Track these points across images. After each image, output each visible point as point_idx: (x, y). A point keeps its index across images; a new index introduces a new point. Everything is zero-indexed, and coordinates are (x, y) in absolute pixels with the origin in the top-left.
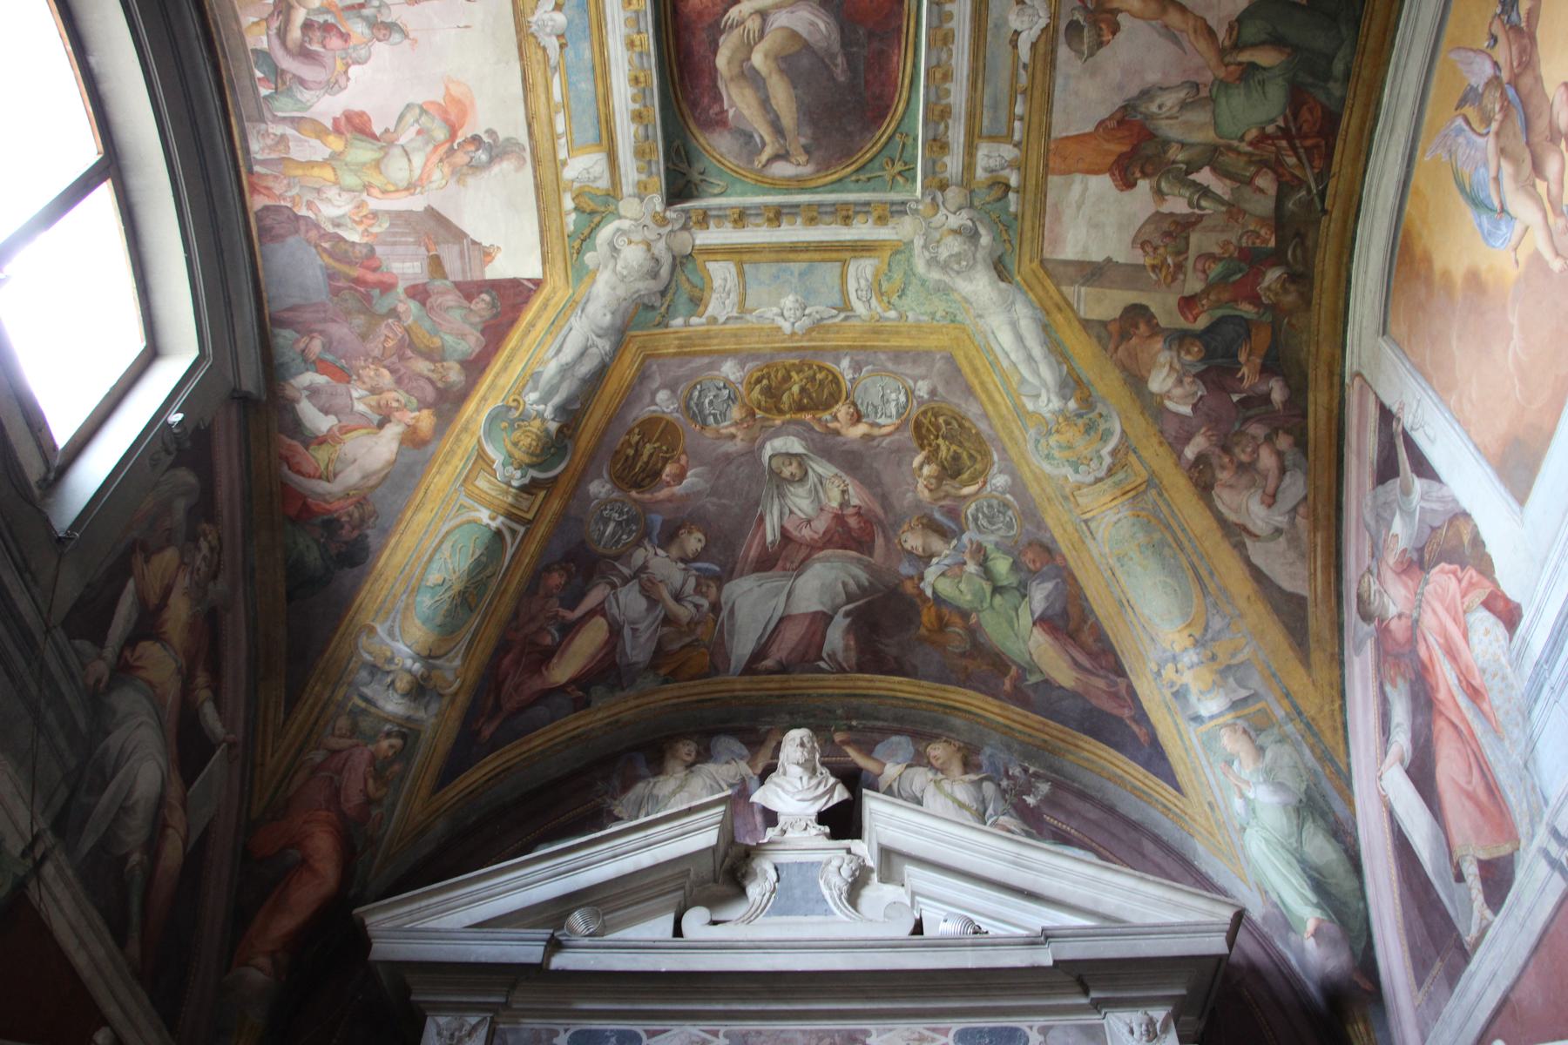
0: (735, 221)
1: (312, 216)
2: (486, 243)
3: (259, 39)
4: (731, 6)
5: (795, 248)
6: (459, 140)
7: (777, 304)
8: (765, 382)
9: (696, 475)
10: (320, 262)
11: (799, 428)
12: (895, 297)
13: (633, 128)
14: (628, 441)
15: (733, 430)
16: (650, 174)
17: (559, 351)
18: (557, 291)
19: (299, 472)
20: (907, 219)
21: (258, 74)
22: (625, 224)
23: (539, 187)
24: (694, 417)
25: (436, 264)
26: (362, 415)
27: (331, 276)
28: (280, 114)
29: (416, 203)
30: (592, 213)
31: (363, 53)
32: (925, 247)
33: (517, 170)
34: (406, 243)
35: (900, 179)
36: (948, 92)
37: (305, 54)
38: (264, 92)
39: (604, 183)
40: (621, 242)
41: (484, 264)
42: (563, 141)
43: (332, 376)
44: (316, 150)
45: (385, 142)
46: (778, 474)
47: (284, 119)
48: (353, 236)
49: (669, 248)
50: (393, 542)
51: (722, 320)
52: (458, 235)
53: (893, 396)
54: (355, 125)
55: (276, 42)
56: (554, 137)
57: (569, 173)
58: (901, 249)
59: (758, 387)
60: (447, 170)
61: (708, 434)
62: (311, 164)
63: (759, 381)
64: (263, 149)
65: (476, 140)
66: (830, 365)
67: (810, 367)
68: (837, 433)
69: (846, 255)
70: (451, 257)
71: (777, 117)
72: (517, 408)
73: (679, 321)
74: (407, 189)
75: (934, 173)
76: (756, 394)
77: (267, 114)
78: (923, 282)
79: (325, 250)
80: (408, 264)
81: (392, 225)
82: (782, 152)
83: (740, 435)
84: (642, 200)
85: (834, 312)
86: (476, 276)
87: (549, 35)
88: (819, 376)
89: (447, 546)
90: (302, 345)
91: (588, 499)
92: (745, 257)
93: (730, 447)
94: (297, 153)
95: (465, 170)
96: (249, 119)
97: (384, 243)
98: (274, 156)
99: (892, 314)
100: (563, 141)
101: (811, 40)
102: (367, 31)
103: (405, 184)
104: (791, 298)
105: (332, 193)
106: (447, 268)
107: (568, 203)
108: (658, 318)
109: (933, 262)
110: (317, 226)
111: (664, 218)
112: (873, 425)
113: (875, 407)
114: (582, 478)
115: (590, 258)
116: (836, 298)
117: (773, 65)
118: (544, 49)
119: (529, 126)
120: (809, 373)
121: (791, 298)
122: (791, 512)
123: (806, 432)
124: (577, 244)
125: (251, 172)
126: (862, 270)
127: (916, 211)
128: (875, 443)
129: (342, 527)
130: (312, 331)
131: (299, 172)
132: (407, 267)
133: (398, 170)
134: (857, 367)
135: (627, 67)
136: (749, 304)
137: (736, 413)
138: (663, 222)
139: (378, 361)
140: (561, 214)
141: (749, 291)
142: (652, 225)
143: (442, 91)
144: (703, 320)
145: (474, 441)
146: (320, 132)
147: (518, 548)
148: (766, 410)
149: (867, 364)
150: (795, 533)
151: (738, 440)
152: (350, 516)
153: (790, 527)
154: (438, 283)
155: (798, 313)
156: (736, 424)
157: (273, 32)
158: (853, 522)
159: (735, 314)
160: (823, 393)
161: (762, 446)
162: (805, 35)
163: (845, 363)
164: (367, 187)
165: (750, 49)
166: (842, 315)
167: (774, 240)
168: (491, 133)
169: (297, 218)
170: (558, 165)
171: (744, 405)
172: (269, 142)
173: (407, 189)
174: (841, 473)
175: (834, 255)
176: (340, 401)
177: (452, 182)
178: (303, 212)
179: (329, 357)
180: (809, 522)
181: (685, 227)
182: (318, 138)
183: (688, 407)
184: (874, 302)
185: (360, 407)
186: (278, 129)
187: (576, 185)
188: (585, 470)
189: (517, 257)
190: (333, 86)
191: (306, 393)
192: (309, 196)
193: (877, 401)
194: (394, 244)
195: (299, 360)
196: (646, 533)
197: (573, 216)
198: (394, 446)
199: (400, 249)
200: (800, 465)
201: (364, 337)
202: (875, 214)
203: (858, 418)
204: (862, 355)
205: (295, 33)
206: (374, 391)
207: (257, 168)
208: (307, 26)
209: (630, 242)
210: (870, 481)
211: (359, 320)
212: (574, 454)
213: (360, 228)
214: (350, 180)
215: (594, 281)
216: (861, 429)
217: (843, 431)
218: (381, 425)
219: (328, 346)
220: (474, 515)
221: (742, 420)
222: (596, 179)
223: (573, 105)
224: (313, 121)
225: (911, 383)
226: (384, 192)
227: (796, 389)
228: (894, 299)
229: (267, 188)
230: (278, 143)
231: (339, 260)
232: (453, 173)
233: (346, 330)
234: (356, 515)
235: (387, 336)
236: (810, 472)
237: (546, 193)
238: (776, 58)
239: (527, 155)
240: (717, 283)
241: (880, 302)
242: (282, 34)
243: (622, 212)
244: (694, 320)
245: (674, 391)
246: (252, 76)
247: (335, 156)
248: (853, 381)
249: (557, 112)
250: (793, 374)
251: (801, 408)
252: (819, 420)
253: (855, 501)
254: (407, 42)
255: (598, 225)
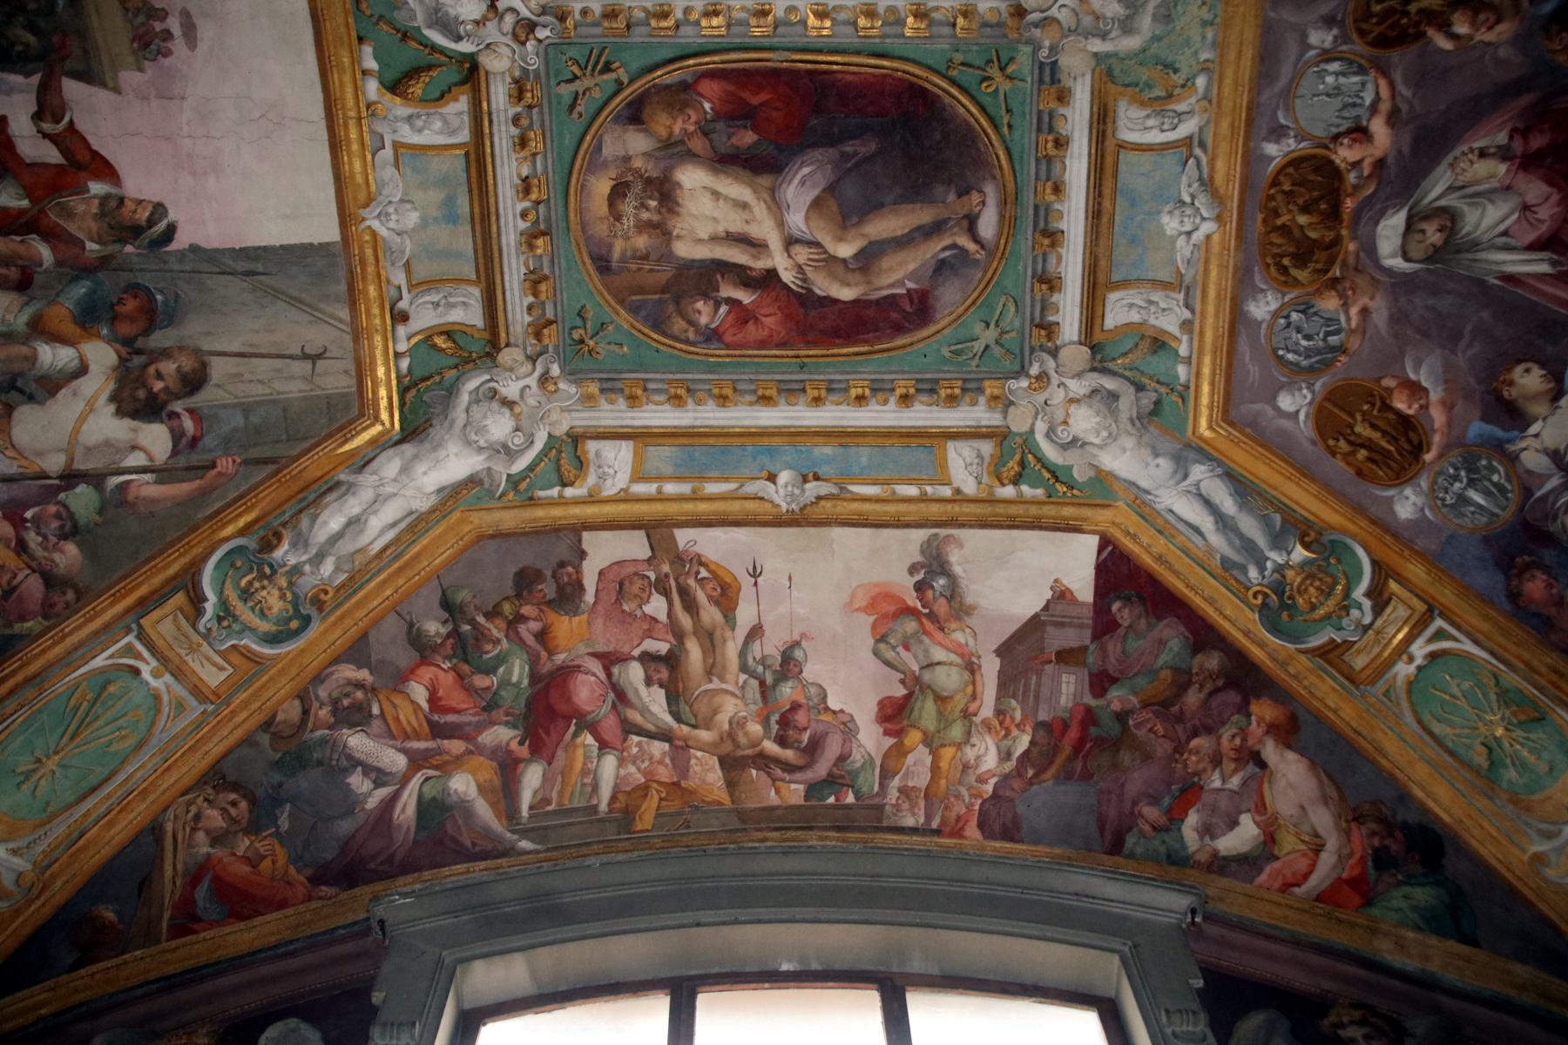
0: (1051, 289)
1: (993, 781)
2: (1049, 594)
3: (795, 792)
4: (780, 280)
5: (1096, 215)
6: (919, 605)
7: (1173, 240)
8: (1286, 262)
9: (1417, 366)
10: (1050, 783)
11: (1366, 216)
12: (1175, 77)
13: (918, 406)
14: (1346, 455)
15: (1354, 311)
16: (980, 391)
17: (1197, 530)
18: (1118, 518)
19: (1306, 876)
20: (1064, 61)
21: (832, 800)
22: (1041, 427)
23: (984, 524)
24: (1327, 365)
25: (1066, 657)
26: (1244, 783)
27: (1067, 776)
28: (876, 788)
29: (991, 667)
30: (1022, 464)
31: (813, 690)
32: (1104, 36)
33: (961, 545)
34: (1039, 684)
35: (1010, 70)
36: (891, 10)
37: (813, 749)
38: (850, 799)
39: (987, 447)
40: (1064, 435)
41: (1074, 601)
42: (929, 489)
43: (1190, 804)
44: (919, 759)
45: (916, 686)
46: (1437, 249)
47: (881, 784)
48: (1023, 742)
49: (1079, 375)
50: (1418, 793)
51: (1187, 314)
52: (1034, 624)
53: (1330, 79)
54: (894, 715)
55: (798, 776)
56: (923, 499)
57: (970, 488)
58: (1107, 73)
59: (1293, 272)
60: (954, 626)
61: (1354, 344)
62: (935, 768)
63: (1284, 270)
64: (914, 814)
65: (920, 587)
66: (1272, 168)
67: (1271, 198)
68: (1380, 163)
69: (1110, 145)
70: (1058, 639)
71: (919, 228)
72: (1266, 596)
73: (1182, 371)
74: (973, 672)
75: (1000, 25)
76: (1302, 275)
77: (876, 801)
78: (1156, 38)
79: (1036, 775)
80: (1064, 690)
81: (1014, 697)
82: (965, 223)
83: (1364, 301)
84: (1012, 403)
85: (1191, 161)
86: (1088, 615)
87: (803, 491)
88: (1287, 187)
89: (1438, 728)
90: (1147, 828)
91: (1419, 524)
92: (1101, 278)
93: (1380, 317)
94: (921, 779)
95: (955, 605)
96: (880, 820)
97: (1036, 710)
98: (922, 804)
99: (1201, 81)
100: (929, 489)
101: (823, 184)
102: (790, 684)
103: (966, 676)
104: (1165, 219)
105: (970, 753)
106: (1074, 644)
107: (1008, 491)
108: (1174, 398)
109: (1127, 26)
110: (1006, 778)
111: (1038, 378)
112: (1374, 109)
113: (1345, 106)
114: (1386, 527)
115: (1079, 475)
116: (1171, 160)
117: (853, 231)
118: (819, 498)
119: (907, 526)
120: (1280, 198)
121: (1165, 219)
122: (1505, 233)
123: (1373, 210)
124: (1061, 488)
125: (938, 832)
126: (1134, 125)
127: (1053, 49)
128: (1404, 108)
129: (1387, 848)
130: (1132, 813)
131: (943, 782)
132: (1068, 689)
133: (948, 678)
134: (1278, 133)
135: (844, 407)
136: (1165, 275)
137: (1329, 304)
138: (1043, 377)
139: (1180, 748)
140: (1020, 501)
141: (1151, 275)
142: (1045, 395)
143: (863, 616)
144: (1185, 338)
145: (1303, 658)
146: (898, 752)
147: (1468, 635)
148: (1331, 262)
149: (1274, 117)
150: (1544, 228)
151: (1372, 305)
152: (1373, 834)
153: (1531, 237)
154: (1091, 659)
155: (1189, 211)
156: (1346, 306)
157: (787, 777)
158: (1538, 142)
159: (1181, 296)
160: (1315, 179)
161: (1389, 271)
162: (816, 192)
163: (1271, 149)
164: (967, 715)
165: (834, 258)
166: (1198, 151)
167: (1081, 240)
168: (912, 570)
169: (995, 795)
170: (959, 497)
171: (1319, 292)
172: (906, 806)
173: (973, 672)
174: (1450, 158)
175: (1109, 160)
176: (1224, 803)
177: (969, 621)
178: (989, 788)
179: (1166, 801)
180: (1526, 208)
181: (1054, 353)
182: (905, 754)
183: (1311, 370)
184: (1182, 107)
185: (1235, 782)
186: (893, 795)
187: (985, 479)
188: (1374, 522)
189: (1073, 562)
190: (848, 728)
191: (1207, 839)
192: (972, 779)
193: (1337, 103)
194: (1037, 697)
195: (1166, 837)
196: (1498, 448)
197: (1025, 488)
198: (1291, 756)
199: (1045, 691)
200: (1428, 216)
201: (1147, 757)
202: (1053, 105)
203: (1360, 133)
204: (1258, 122)
205: (789, 754)
206: (1216, 761)
207: (935, 825)
208: (782, 741)
209: (1065, 423)
210: (1472, 113)
211: (1126, 757)
212: (1345, 532)
213: (1015, 732)
214: (956, 732)
215: (1110, 474)
216: (1378, 127)
217: (1378, 153)
218: (1263, 765)
219: (1155, 800)
220: (1400, 682)
221: (1341, 296)
222: (980, 456)
223: (885, 475)
224: (886, 756)
225: (1312, 53)
226: (974, 697)
227: (1302, 220)
228: (1178, 79)
229: (958, 819)
230: (908, 797)
231: (1051, 763)
232: (959, 619)
233: (1136, 775)
234: (1373, 826)
235: (1148, 728)
236: (1443, 203)
237: (995, 517)
238: (844, 228)
239: (943, 532)
240: (1135, 317)
241: (1180, 99)
242: (790, 768)
243: (1025, 428)
244: (1183, 350)
245: (1281, 387)
246: (833, 806)
247: (928, 741)
248: (1300, 137)
249: (894, 493)
250: (1279, 222)
251: (1334, 214)
252: (1356, 188)
253: (1502, 138)
254: (804, 643)
255: (1039, 460)
